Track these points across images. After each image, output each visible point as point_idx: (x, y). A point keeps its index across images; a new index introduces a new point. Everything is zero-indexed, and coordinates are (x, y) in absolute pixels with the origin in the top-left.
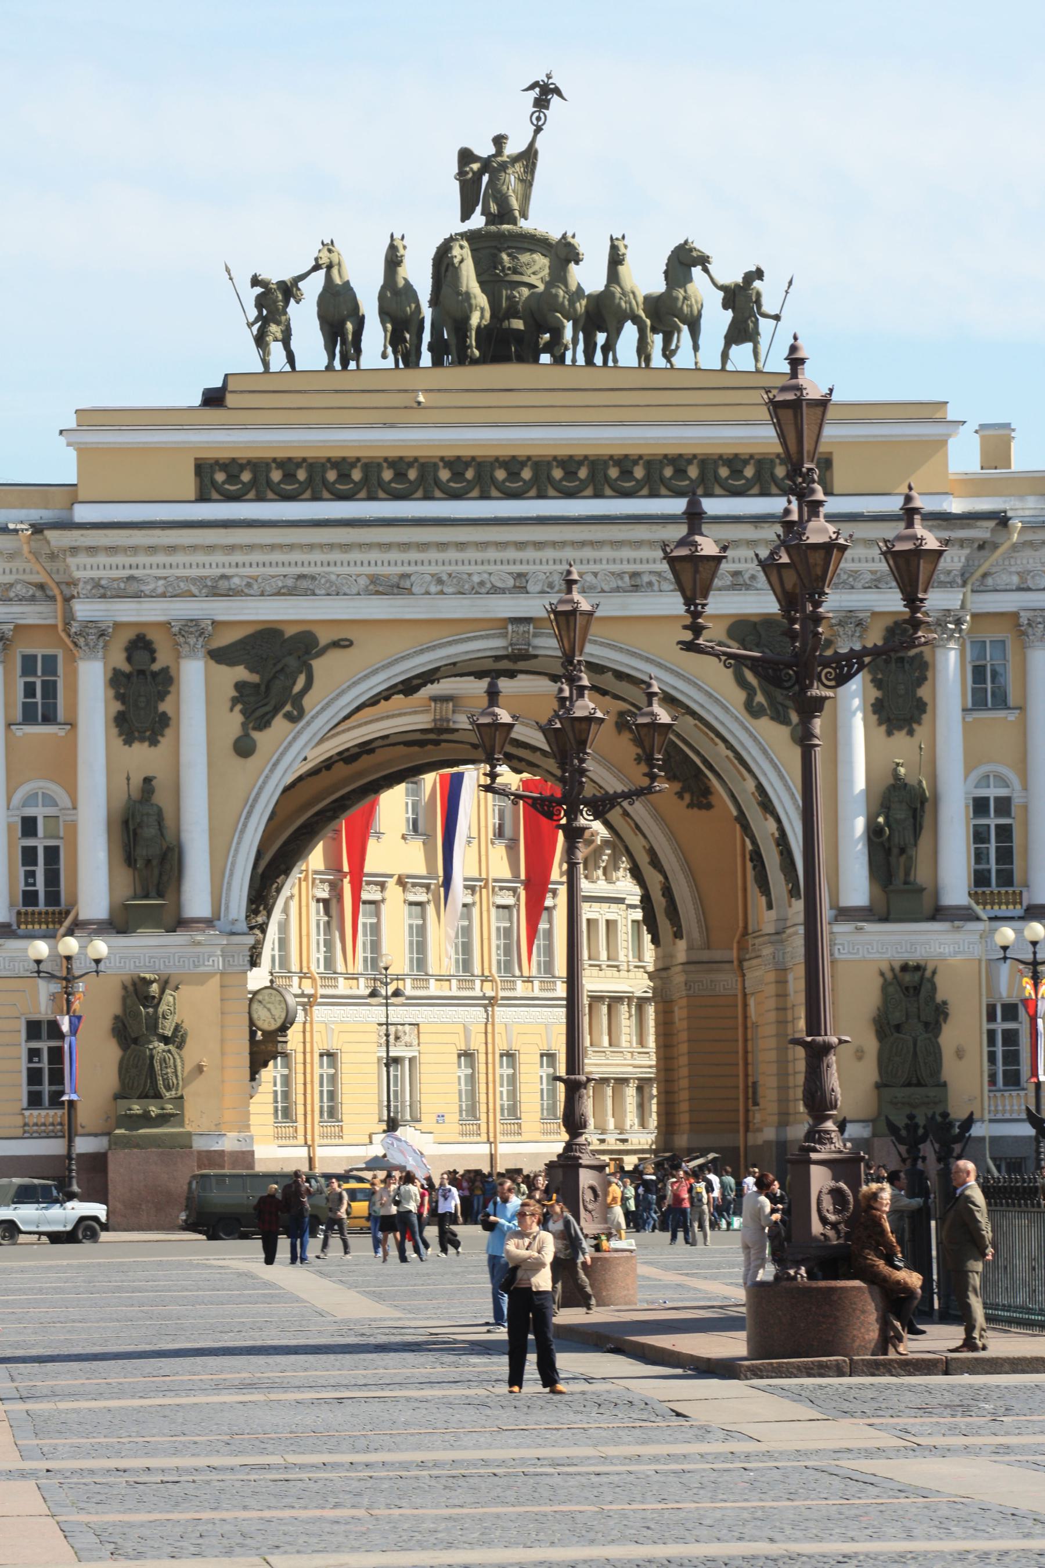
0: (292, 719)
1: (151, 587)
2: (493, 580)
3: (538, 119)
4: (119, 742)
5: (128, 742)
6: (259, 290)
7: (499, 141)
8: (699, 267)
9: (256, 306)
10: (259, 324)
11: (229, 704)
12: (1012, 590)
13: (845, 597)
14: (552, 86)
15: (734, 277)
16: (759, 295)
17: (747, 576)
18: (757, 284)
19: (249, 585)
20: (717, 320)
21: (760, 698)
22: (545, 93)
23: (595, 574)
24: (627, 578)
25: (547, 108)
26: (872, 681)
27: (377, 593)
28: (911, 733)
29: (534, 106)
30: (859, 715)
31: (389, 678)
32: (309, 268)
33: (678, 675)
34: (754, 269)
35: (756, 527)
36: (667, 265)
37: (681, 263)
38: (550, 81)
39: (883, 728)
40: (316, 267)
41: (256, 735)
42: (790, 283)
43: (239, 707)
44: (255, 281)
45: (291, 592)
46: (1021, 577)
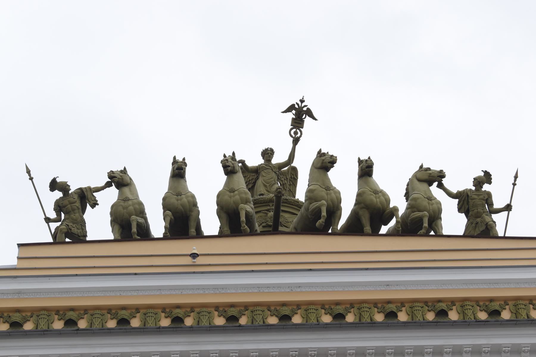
3: (296, 133)
6: (58, 194)
7: (268, 154)
8: (436, 184)
9: (55, 209)
10: (58, 224)
14: (305, 109)
15: (467, 184)
16: (489, 195)
18: (486, 187)
20: (453, 221)
22: (300, 114)
25: (302, 128)
29: (291, 125)
32: (103, 184)
34: (482, 174)
36: (407, 189)
37: (420, 180)
38: (303, 104)
40: (108, 185)
42: (516, 177)
44: (54, 185)
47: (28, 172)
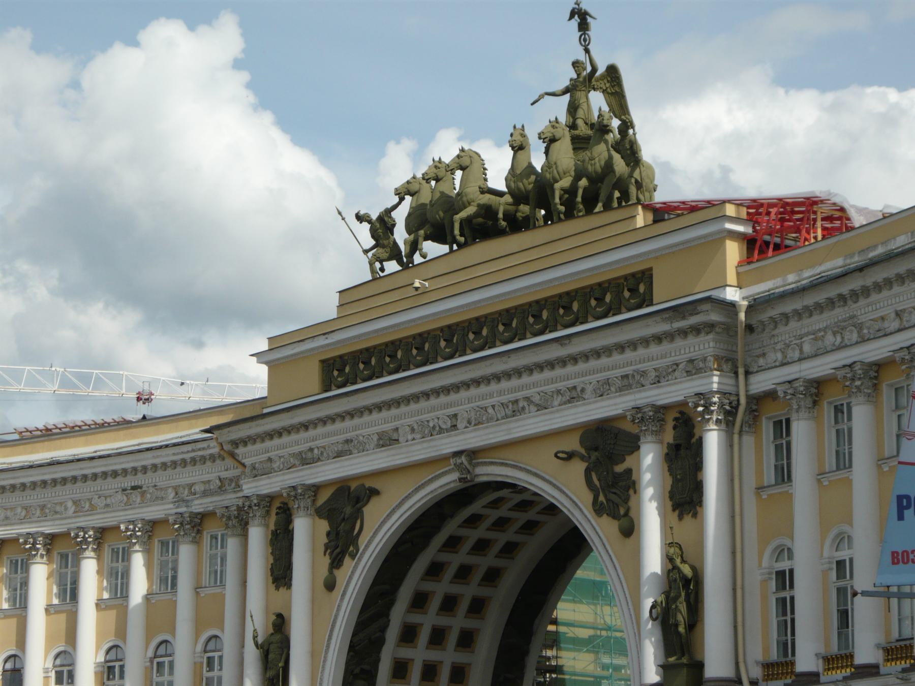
0: (353, 557)
1: (278, 464)
2: (441, 423)
3: (585, 40)
4: (272, 587)
5: (277, 588)
11: (322, 549)
12: (776, 367)
13: (638, 396)
17: (579, 389)
19: (322, 453)
21: (602, 498)
22: (581, 18)
23: (493, 407)
24: (510, 406)
26: (669, 470)
27: (383, 446)
28: (695, 515)
29: (579, 31)
30: (654, 505)
31: (401, 516)
33: (554, 486)
35: (562, 345)
39: (677, 512)
41: (336, 572)
43: (329, 551)
44: (360, 218)
45: (339, 455)
46: (783, 352)
47: (340, 213)
